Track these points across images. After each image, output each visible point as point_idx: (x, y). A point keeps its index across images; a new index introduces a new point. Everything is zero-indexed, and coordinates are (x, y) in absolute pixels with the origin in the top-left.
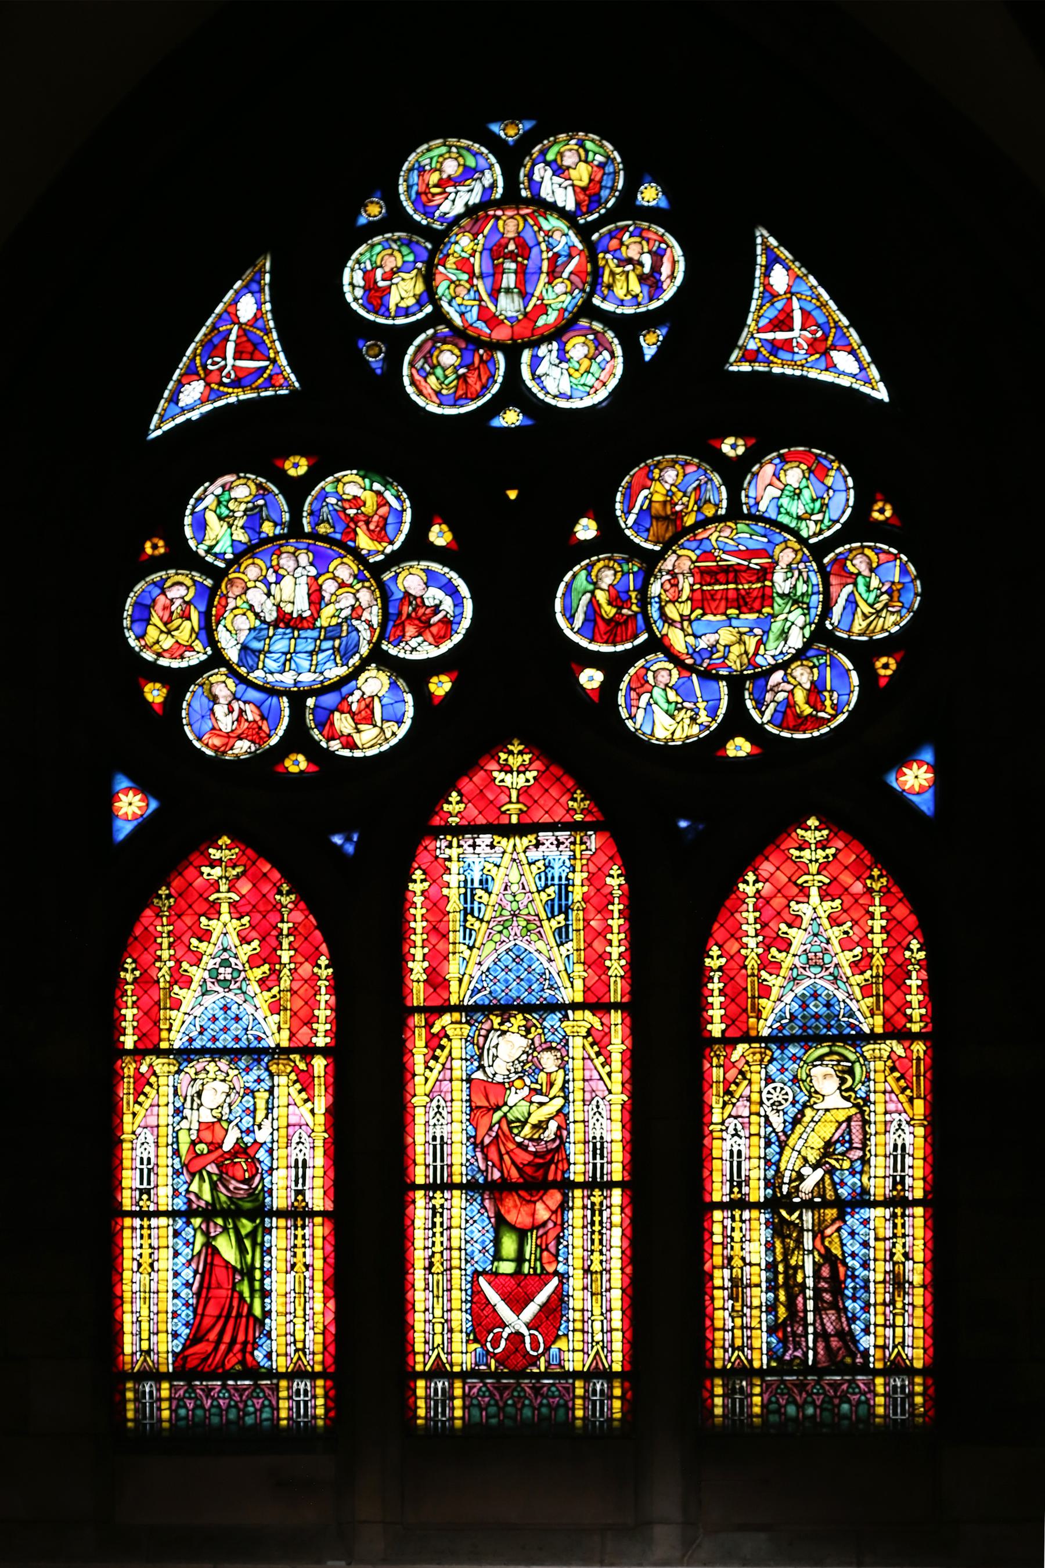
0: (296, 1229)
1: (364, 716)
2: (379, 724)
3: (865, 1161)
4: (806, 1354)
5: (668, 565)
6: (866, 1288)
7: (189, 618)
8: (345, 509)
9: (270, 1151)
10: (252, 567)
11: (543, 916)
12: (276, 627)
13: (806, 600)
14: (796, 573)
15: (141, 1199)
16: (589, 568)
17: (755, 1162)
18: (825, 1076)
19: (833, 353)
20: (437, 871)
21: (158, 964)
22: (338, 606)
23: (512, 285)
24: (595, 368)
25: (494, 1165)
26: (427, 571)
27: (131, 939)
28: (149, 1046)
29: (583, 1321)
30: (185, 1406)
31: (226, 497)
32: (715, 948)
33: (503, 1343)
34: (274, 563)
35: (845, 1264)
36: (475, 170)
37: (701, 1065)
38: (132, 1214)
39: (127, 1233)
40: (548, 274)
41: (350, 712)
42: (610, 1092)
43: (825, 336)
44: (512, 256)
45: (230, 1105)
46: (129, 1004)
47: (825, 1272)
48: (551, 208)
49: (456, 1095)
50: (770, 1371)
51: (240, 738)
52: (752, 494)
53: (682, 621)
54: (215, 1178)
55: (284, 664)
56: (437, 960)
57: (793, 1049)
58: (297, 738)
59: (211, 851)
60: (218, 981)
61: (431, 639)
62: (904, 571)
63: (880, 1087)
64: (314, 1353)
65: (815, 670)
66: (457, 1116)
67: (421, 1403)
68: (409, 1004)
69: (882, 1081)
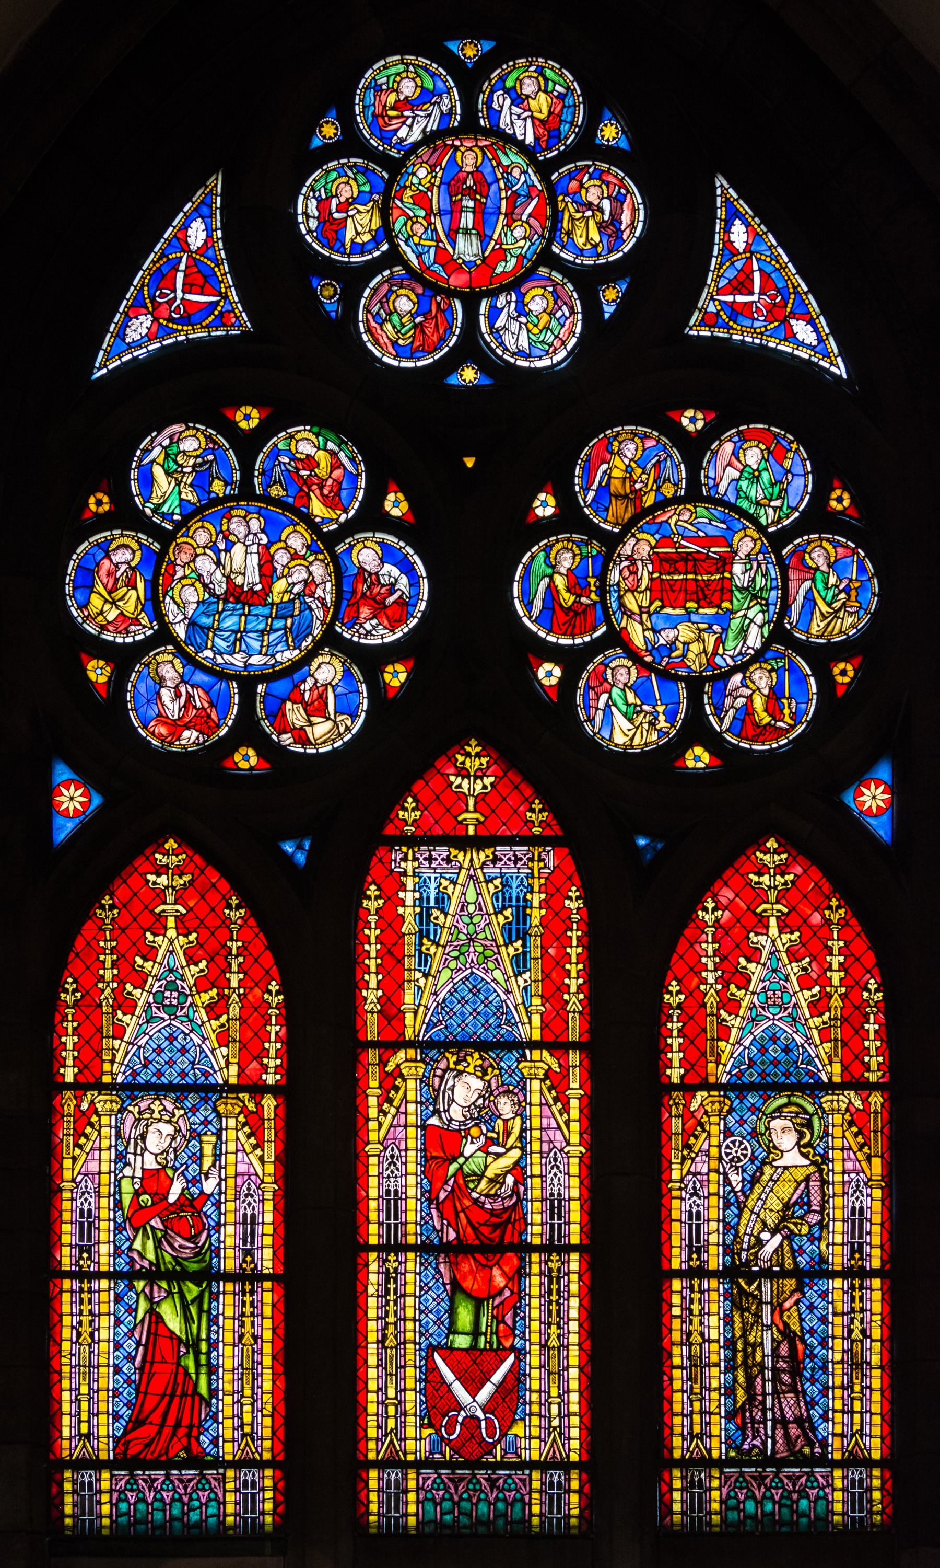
0: (244, 1295)
1: (316, 708)
2: (332, 717)
3: (822, 1225)
4: (764, 1443)
5: (627, 549)
6: (824, 1369)
7: (135, 588)
8: (298, 470)
9: (218, 1204)
10: (201, 532)
11: (501, 941)
12: (226, 601)
13: (765, 595)
14: (755, 564)
15: (81, 1258)
16: (547, 549)
17: (713, 1226)
18: (784, 1130)
19: (793, 322)
20: (392, 886)
21: (100, 985)
22: (290, 580)
23: (470, 226)
24: (554, 323)
25: (449, 1225)
26: (382, 544)
27: (72, 955)
28: (90, 1082)
29: (541, 1404)
30: (126, 1500)
31: (175, 450)
32: (674, 983)
33: (458, 1428)
34: (224, 528)
35: (803, 1341)
36: (433, 93)
37: (660, 1115)
38: (71, 1275)
39: (66, 1297)
40: (506, 215)
41: (302, 701)
42: (568, 1144)
43: (785, 301)
44: (470, 192)
45: (175, 1150)
46: (70, 1031)
47: (784, 1350)
48: (510, 140)
49: (411, 1144)
50: (730, 1462)
51: (187, 727)
52: (712, 474)
53: (641, 613)
54: (159, 1234)
55: (234, 644)
57: (752, 1099)
58: (247, 731)
59: (157, 856)
60: (164, 1006)
61: (386, 623)
62: (862, 569)
63: (838, 1143)
64: (262, 1439)
65: (774, 675)
66: (411, 1167)
67: (373, 1497)
68: (361, 1038)
69: (841, 1136)
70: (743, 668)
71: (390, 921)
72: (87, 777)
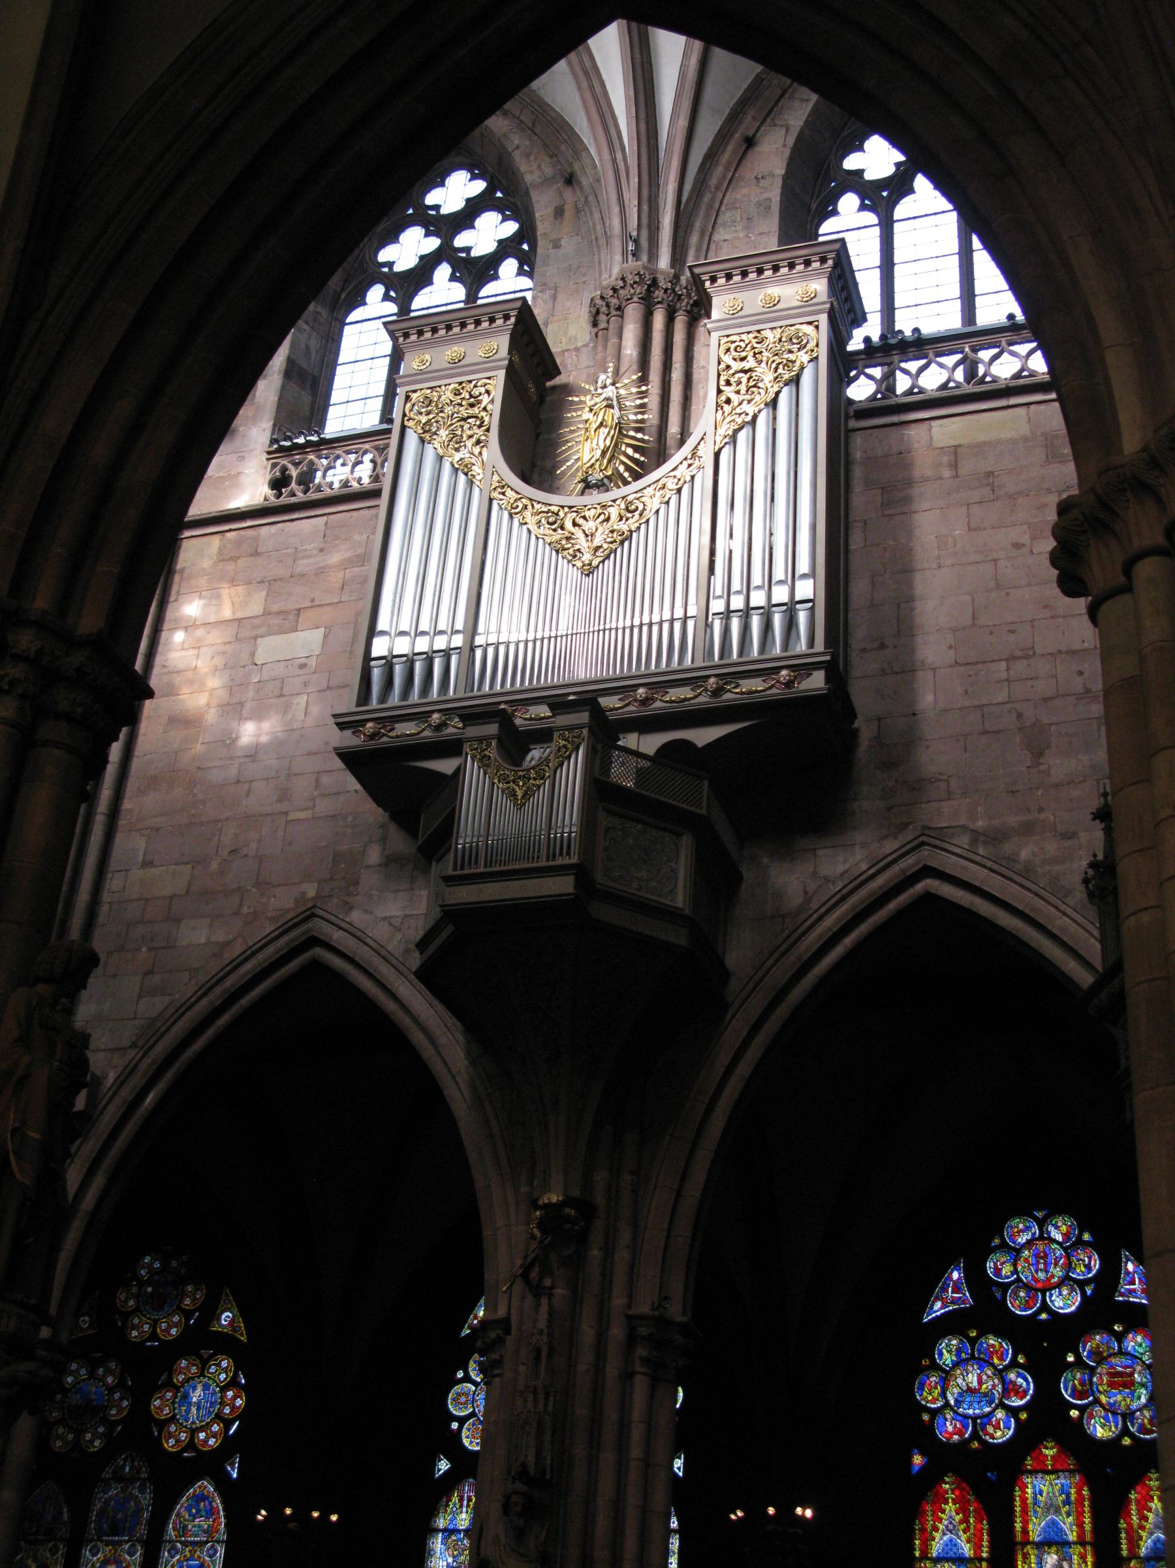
1: (997, 1427)
5: (1099, 1370)
56: (1025, 1523)
58: (975, 1436)
70: (1140, 1410)
71: (1024, 1500)
72: (922, 1454)
